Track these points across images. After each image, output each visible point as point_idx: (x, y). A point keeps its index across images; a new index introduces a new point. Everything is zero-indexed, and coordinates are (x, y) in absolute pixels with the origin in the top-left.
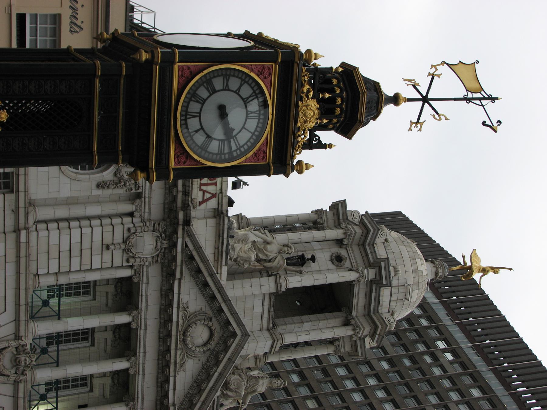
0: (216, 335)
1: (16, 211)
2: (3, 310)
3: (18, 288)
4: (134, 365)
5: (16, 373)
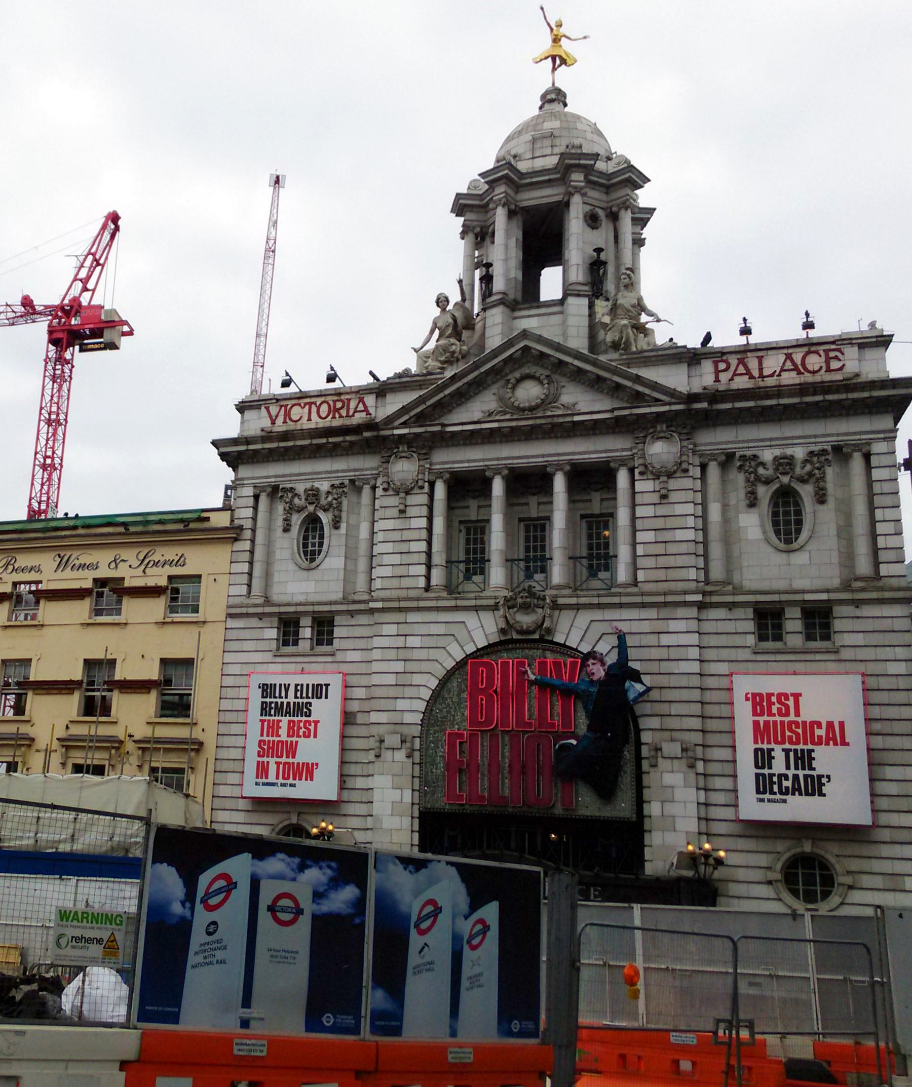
0: (528, 371)
1: (351, 614)
2: (462, 625)
3: (438, 609)
4: (559, 467)
5: (543, 608)
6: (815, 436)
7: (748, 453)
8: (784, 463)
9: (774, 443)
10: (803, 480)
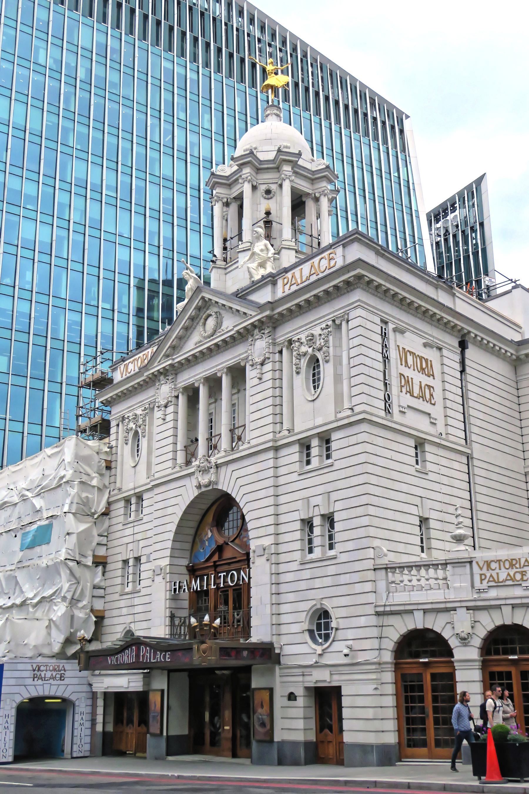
6: (324, 316)
7: (295, 338)
8: (311, 339)
9: (308, 327)
10: (319, 350)
